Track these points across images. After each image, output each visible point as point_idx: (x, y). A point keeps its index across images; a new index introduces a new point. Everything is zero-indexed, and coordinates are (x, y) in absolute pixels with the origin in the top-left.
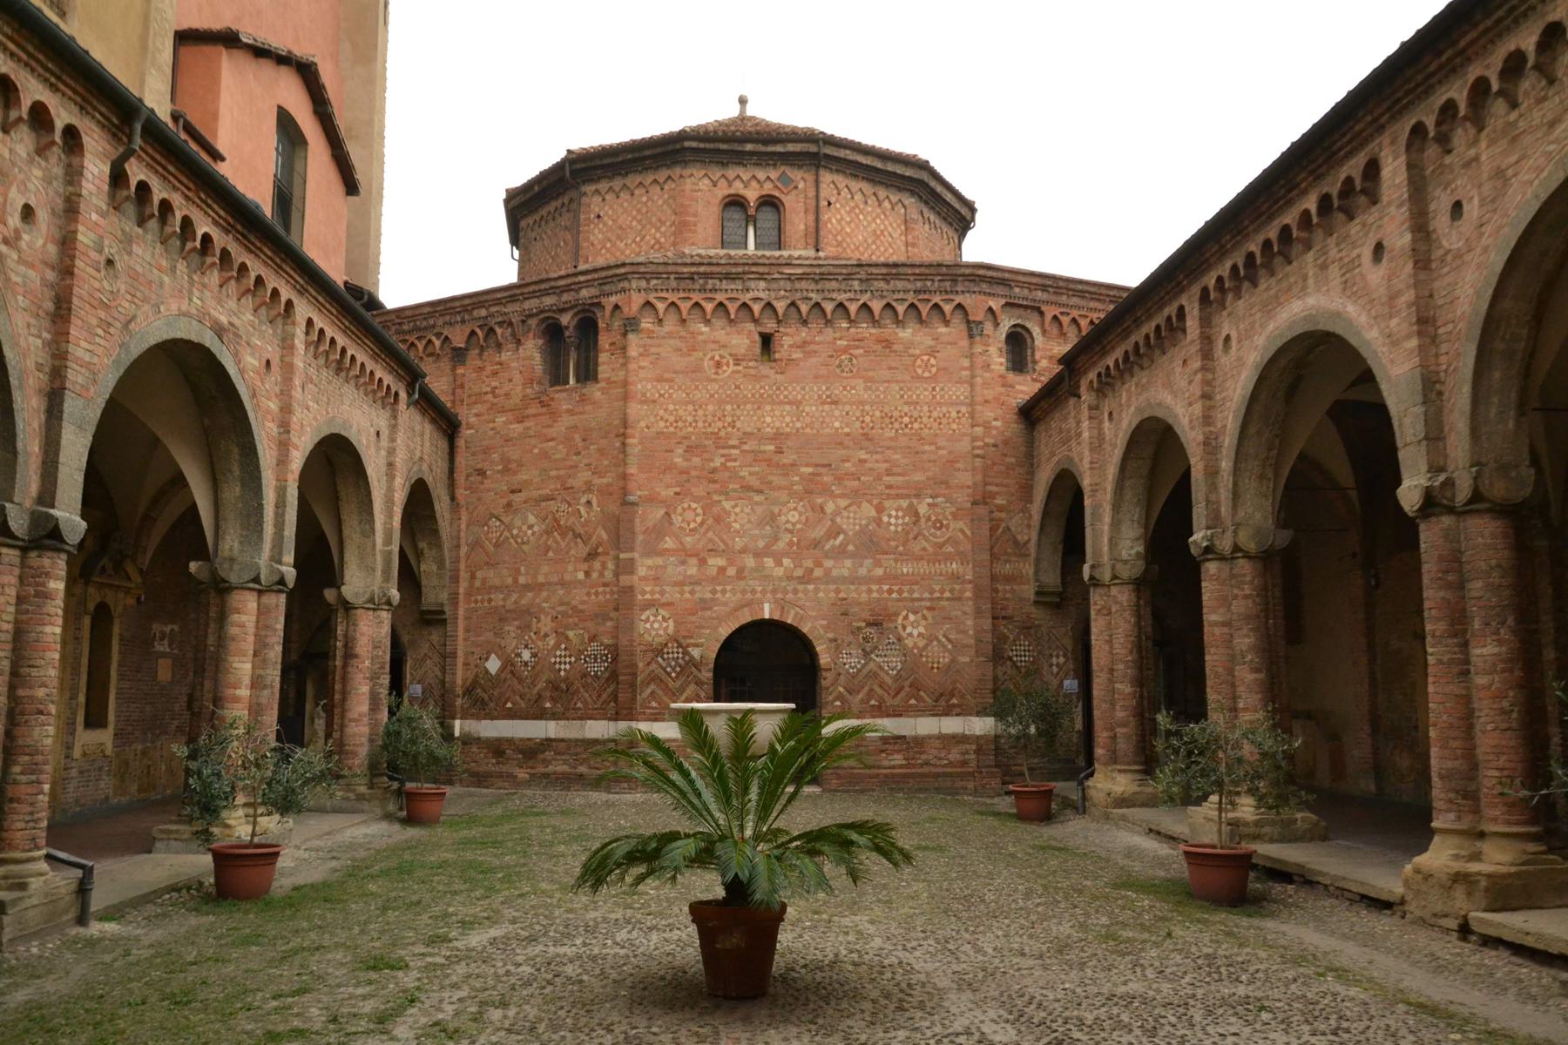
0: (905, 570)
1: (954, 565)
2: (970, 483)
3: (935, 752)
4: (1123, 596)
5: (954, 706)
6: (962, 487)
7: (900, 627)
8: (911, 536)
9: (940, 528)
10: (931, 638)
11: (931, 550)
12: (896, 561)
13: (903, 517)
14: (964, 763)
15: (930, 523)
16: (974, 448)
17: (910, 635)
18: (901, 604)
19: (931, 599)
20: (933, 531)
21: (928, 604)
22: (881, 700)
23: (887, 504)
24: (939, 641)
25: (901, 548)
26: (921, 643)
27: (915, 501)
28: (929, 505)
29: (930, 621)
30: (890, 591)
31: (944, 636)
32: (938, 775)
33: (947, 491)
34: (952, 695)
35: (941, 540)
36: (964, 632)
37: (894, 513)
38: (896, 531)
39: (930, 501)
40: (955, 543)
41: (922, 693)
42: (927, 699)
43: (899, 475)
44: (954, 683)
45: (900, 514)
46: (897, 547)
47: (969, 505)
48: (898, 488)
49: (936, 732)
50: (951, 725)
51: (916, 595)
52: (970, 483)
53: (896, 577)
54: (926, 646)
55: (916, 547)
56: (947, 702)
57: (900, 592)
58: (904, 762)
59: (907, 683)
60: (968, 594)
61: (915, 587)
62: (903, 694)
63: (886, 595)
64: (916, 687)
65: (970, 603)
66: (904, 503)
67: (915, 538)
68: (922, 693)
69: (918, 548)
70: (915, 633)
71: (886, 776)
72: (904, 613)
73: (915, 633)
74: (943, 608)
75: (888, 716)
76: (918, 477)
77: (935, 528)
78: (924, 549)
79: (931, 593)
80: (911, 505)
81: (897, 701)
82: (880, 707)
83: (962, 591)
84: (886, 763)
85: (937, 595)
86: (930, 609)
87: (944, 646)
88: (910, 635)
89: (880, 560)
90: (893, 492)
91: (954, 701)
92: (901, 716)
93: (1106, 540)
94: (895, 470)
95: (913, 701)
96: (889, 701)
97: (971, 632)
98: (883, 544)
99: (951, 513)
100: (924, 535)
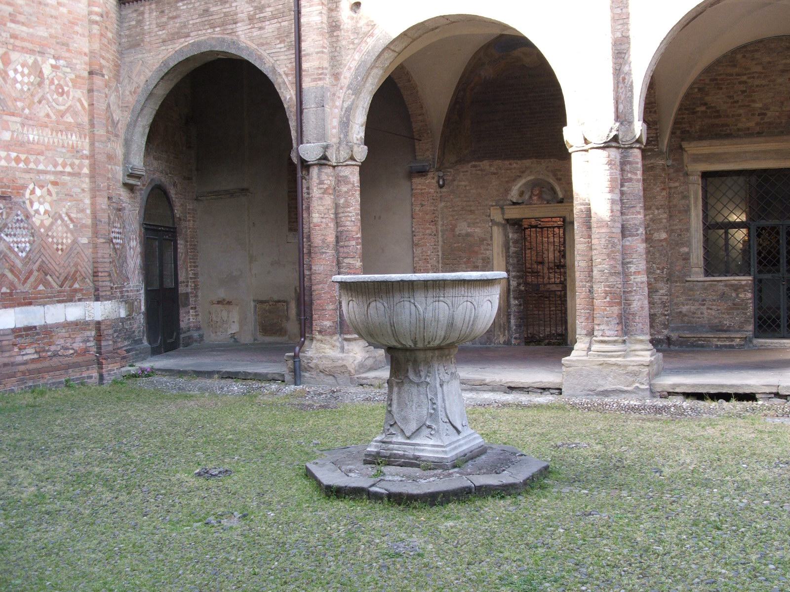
0: (31, 137)
1: (74, 137)
2: (87, 50)
3: (62, 342)
4: (353, 176)
5: (76, 291)
6: (80, 53)
7: (27, 202)
8: (36, 99)
9: (62, 94)
10: (57, 217)
11: (54, 117)
12: (23, 125)
13: (29, 75)
14: (86, 351)
15: (53, 87)
16: (90, 13)
17: (37, 211)
18: (27, 176)
19: (55, 173)
20: (55, 96)
21: (52, 178)
22: (12, 286)
23: (14, 56)
24: (63, 220)
25: (27, 111)
26: (47, 223)
27: (39, 59)
28: (53, 66)
29: (54, 197)
30: (17, 160)
31: (67, 214)
32: (68, 367)
33: (67, 55)
34: (74, 279)
35: (62, 108)
36: (83, 211)
37: (19, 68)
38: (22, 90)
39: (53, 62)
40: (75, 114)
41: (49, 277)
42: (54, 285)
43: (23, 24)
44: (76, 265)
45: (26, 71)
46: (23, 109)
47: (86, 74)
48: (23, 40)
49: (62, 320)
50: (74, 312)
51: (41, 167)
52: (87, 50)
53: (22, 144)
54: (52, 224)
55: (42, 111)
56: (70, 287)
57: (27, 162)
58: (36, 356)
59: (35, 267)
60: (86, 171)
61: (41, 158)
62: (32, 279)
63: (13, 164)
64: (44, 270)
65: (87, 180)
66: (30, 60)
67: (40, 102)
68: (49, 277)
69: (42, 114)
70: (42, 211)
71: (23, 373)
72: (31, 186)
73: (42, 211)
74: (64, 184)
75: (20, 304)
76: (42, 32)
77: (58, 93)
78: (48, 116)
79: (55, 166)
80: (35, 62)
81: (27, 287)
82: (11, 294)
83: (81, 167)
84: (19, 359)
85: (60, 168)
86: (55, 183)
87: (67, 226)
88: (37, 211)
89: (7, 122)
90: (18, 43)
91: (76, 286)
92: (30, 304)
93: (335, 122)
94: (21, 18)
95: (41, 287)
96: (21, 288)
97: (88, 211)
98: (10, 103)
99: (71, 80)
100: (48, 102)
